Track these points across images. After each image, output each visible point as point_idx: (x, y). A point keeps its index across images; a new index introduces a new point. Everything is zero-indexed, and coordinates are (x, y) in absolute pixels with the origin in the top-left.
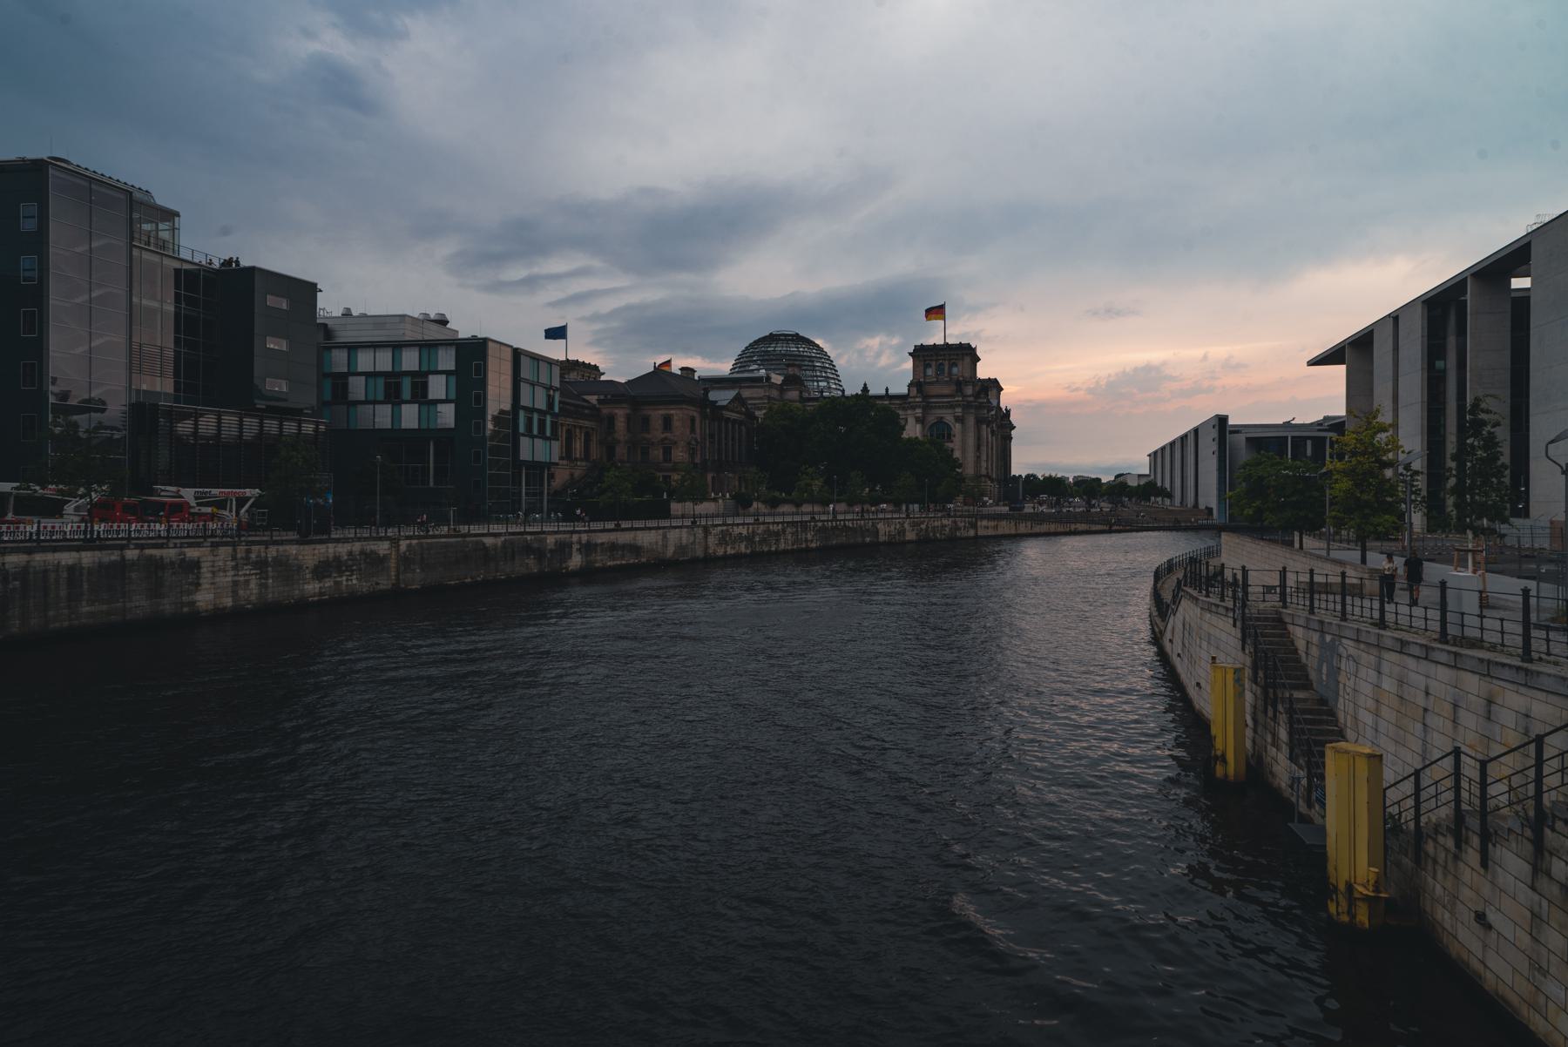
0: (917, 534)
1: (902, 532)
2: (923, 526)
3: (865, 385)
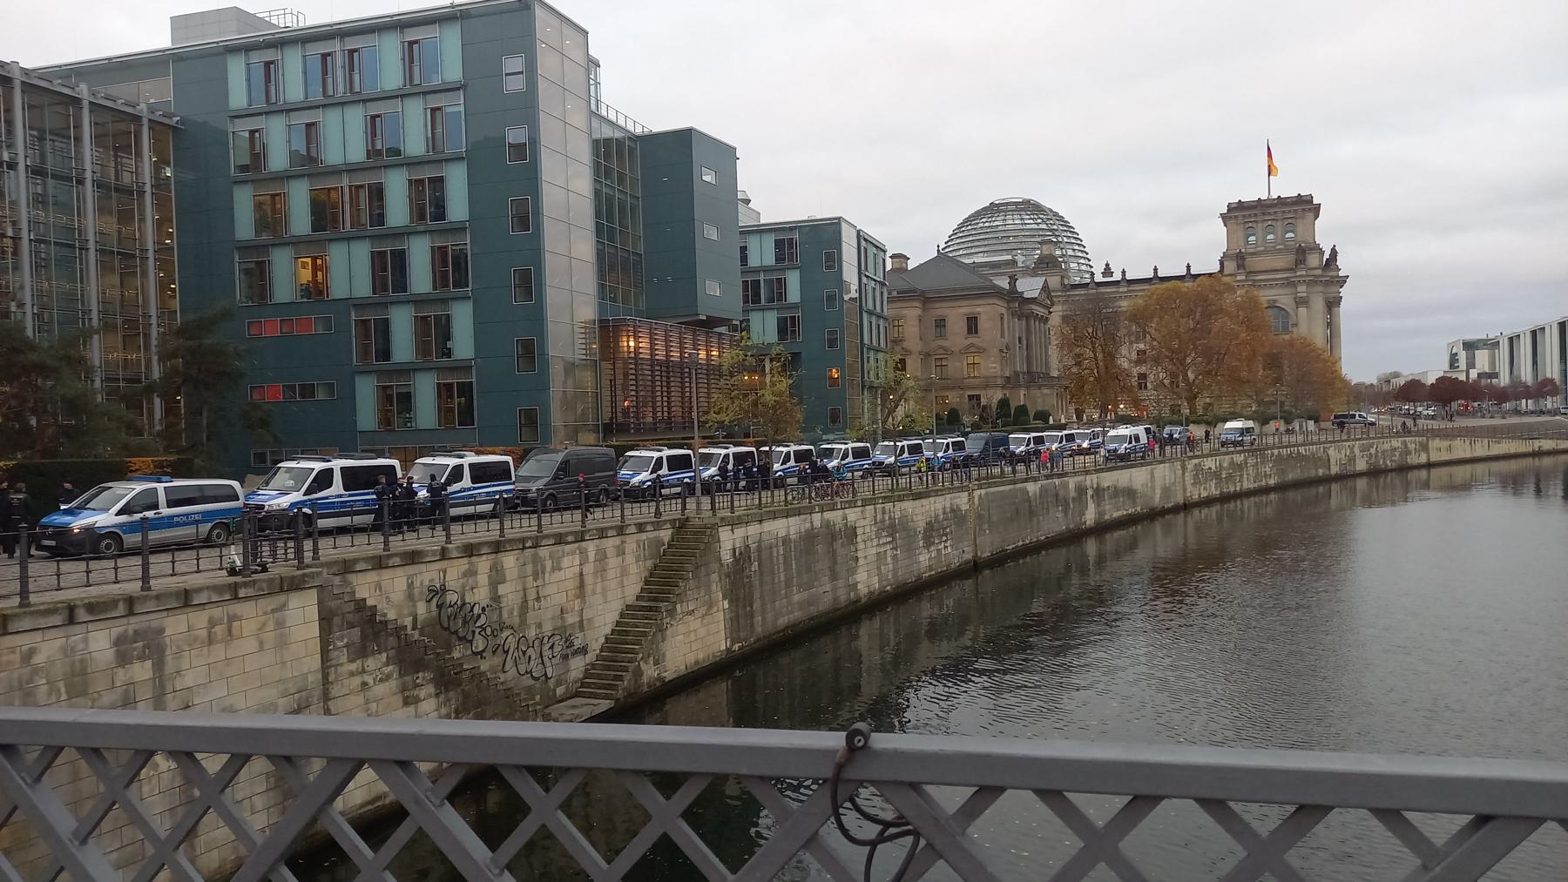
0: (1367, 463)
1: (1352, 460)
2: (1373, 451)
3: (1107, 265)
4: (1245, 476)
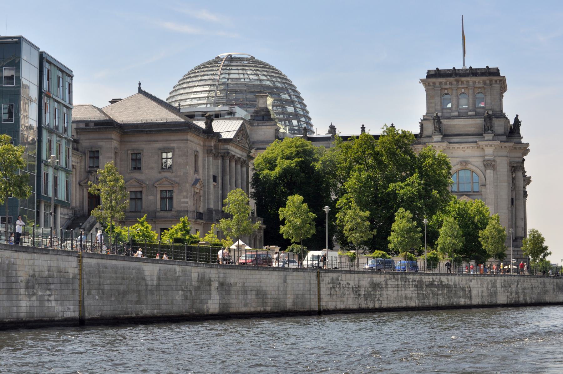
4: (385, 296)
